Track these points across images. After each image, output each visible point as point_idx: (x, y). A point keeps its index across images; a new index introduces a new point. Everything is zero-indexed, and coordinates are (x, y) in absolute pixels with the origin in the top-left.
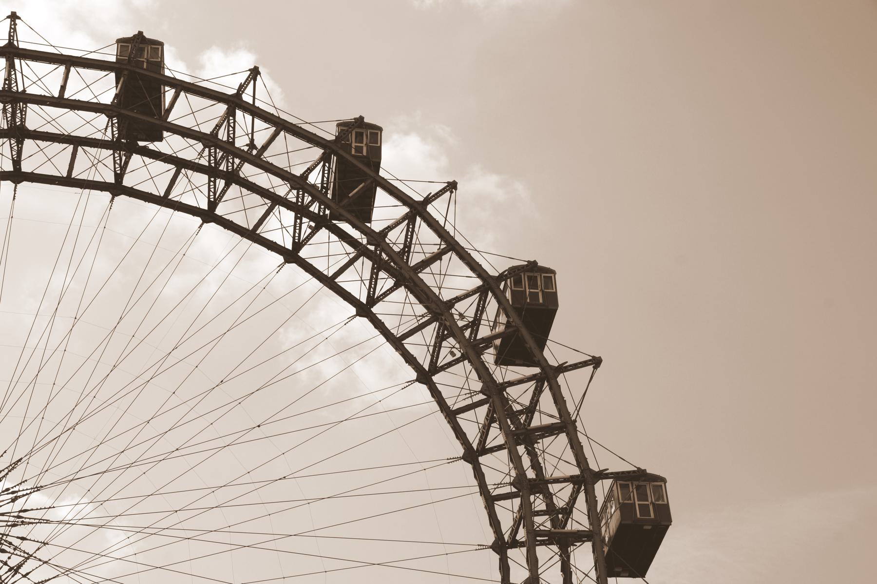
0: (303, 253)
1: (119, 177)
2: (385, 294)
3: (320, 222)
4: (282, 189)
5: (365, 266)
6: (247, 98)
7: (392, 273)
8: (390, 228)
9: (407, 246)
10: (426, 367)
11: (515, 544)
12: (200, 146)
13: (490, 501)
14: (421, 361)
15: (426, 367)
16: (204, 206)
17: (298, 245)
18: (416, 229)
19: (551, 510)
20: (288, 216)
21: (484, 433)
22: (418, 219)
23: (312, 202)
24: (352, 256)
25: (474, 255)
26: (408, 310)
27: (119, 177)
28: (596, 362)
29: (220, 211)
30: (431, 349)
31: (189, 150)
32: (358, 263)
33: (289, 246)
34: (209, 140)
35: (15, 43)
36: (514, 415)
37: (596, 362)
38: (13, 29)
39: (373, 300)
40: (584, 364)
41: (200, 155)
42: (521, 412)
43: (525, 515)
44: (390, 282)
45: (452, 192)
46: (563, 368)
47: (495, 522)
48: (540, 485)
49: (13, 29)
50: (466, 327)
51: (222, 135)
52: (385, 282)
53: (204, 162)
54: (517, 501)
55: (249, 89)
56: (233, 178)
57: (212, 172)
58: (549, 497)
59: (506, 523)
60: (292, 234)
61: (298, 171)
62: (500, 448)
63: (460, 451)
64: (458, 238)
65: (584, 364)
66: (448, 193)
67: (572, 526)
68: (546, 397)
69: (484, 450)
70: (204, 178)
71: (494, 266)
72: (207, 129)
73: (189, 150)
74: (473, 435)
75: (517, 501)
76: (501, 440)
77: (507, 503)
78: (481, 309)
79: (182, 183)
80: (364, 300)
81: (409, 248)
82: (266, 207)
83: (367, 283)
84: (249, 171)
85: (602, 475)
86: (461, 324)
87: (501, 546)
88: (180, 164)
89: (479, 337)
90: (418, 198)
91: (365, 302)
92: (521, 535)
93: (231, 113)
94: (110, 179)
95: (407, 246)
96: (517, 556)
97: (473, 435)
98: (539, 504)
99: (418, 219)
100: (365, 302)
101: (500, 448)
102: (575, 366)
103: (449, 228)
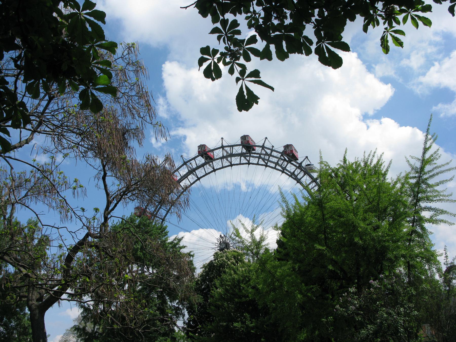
11: (267, 163)
13: (258, 164)
19: (265, 155)
43: (264, 160)
47: (262, 165)
48: (260, 154)
58: (263, 154)
59: (263, 163)
62: (250, 158)
63: (247, 165)
75: (261, 160)
87: (266, 166)
92: (266, 162)
96: (269, 164)
97: (245, 161)
101: (250, 158)
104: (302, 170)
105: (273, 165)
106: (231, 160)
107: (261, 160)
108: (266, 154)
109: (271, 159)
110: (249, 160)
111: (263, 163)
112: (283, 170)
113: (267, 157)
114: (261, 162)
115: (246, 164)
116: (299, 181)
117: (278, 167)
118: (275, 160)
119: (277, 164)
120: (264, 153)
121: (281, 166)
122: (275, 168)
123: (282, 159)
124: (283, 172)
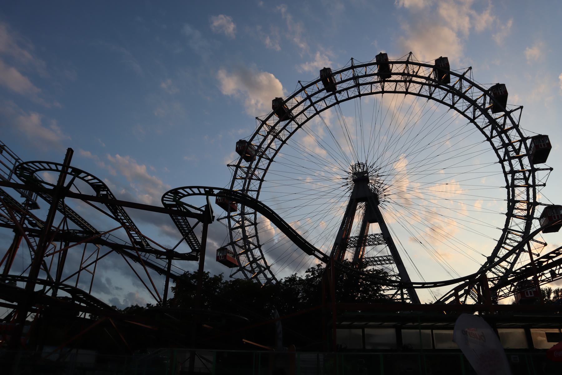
1: (383, 89)
2: (457, 101)
3: (436, 87)
4: (424, 81)
5: (450, 95)
6: (410, 61)
7: (458, 95)
8: (455, 84)
10: (472, 118)
11: (505, 160)
12: (401, 76)
13: (496, 150)
15: (472, 118)
16: (405, 91)
17: (431, 94)
20: (427, 87)
21: (492, 132)
22: (462, 80)
23: (432, 83)
24: (446, 93)
25: (480, 86)
26: (464, 104)
27: (383, 89)
28: (521, 107)
29: (409, 91)
30: (473, 113)
31: (398, 78)
32: (448, 95)
33: (429, 95)
34: (403, 74)
35: (354, 65)
36: (500, 127)
37: (521, 107)
38: (352, 61)
39: (454, 104)
40: (518, 109)
41: (402, 78)
42: (501, 125)
43: (507, 153)
44: (458, 98)
45: (471, 70)
46: (512, 111)
47: (499, 156)
48: (511, 144)
49: (352, 61)
50: (482, 105)
51: (406, 72)
52: (456, 98)
53: (403, 79)
54: (504, 149)
55: (410, 58)
56: (411, 81)
57: (405, 81)
58: (513, 147)
59: (502, 156)
61: (427, 76)
62: (497, 136)
64: (475, 82)
65: (518, 109)
66: (470, 70)
67: (521, 154)
68: (508, 120)
69: (492, 137)
70: (403, 83)
71: (487, 87)
72: (402, 71)
73: (398, 78)
74: (488, 133)
75: (504, 149)
76: (496, 134)
77: (501, 150)
78: (485, 100)
79: (398, 86)
80: (452, 104)
82: (421, 87)
83: (452, 100)
84: (414, 79)
85: (528, 138)
86: (480, 105)
87: (501, 161)
88: (396, 81)
89: (486, 108)
90: (461, 74)
92: (506, 158)
93: (407, 65)
94: (381, 90)
95: (461, 88)
96: (506, 164)
97: (488, 133)
98: (510, 148)
99: (462, 80)
101: (497, 136)
102: (515, 110)
103: (472, 80)
104: (528, 210)
105: (508, 169)
106: (479, 116)
107: (504, 151)
108: (517, 151)
109: (515, 162)
110: (494, 137)
111: (502, 156)
112: (511, 187)
113: (512, 154)
114: (502, 152)
115: (486, 136)
116: (510, 215)
117: (509, 177)
118: (517, 167)
119: (513, 172)
120: (517, 147)
121: (513, 179)
122: (506, 174)
123: (524, 174)
124: (508, 187)
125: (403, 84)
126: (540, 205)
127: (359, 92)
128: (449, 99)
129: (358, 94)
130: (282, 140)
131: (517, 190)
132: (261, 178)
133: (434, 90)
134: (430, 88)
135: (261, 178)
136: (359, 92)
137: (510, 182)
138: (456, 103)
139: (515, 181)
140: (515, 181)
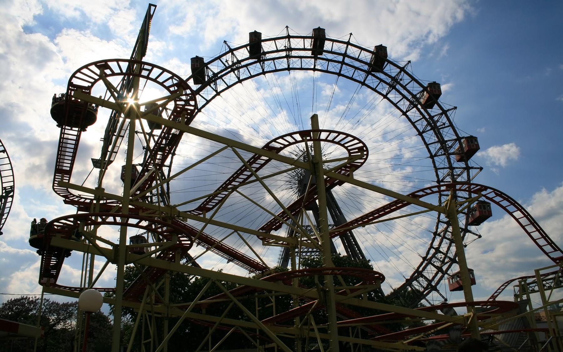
0: (424, 135)
1: (387, 94)
5: (439, 145)
9: (451, 147)
10: (440, 180)
11: (439, 235)
12: (411, 96)
14: (440, 177)
15: (440, 180)
18: (456, 144)
20: (425, 123)
22: (458, 142)
24: (436, 141)
26: (443, 163)
32: (436, 144)
34: (414, 96)
50: (456, 175)
57: (411, 103)
60: (424, 128)
75: (445, 226)
79: (402, 102)
80: (433, 154)
81: (452, 147)
82: (420, 118)
83: (437, 150)
86: (455, 174)
87: (436, 234)
91: (433, 155)
96: (438, 239)
99: (458, 142)
100: (433, 155)
104: (425, 289)
105: (436, 244)
111: (439, 231)
112: (427, 260)
117: (432, 251)
118: (444, 248)
119: (438, 250)
121: (434, 256)
122: (431, 247)
124: (424, 259)
125: (408, 103)
126: (437, 292)
127: (365, 81)
128: (434, 148)
129: (363, 81)
130: (263, 70)
131: (430, 267)
132: (218, 91)
133: (429, 130)
134: (427, 126)
135: (218, 91)
136: (365, 81)
137: (429, 256)
138: (437, 156)
139: (434, 258)
140: (434, 258)
